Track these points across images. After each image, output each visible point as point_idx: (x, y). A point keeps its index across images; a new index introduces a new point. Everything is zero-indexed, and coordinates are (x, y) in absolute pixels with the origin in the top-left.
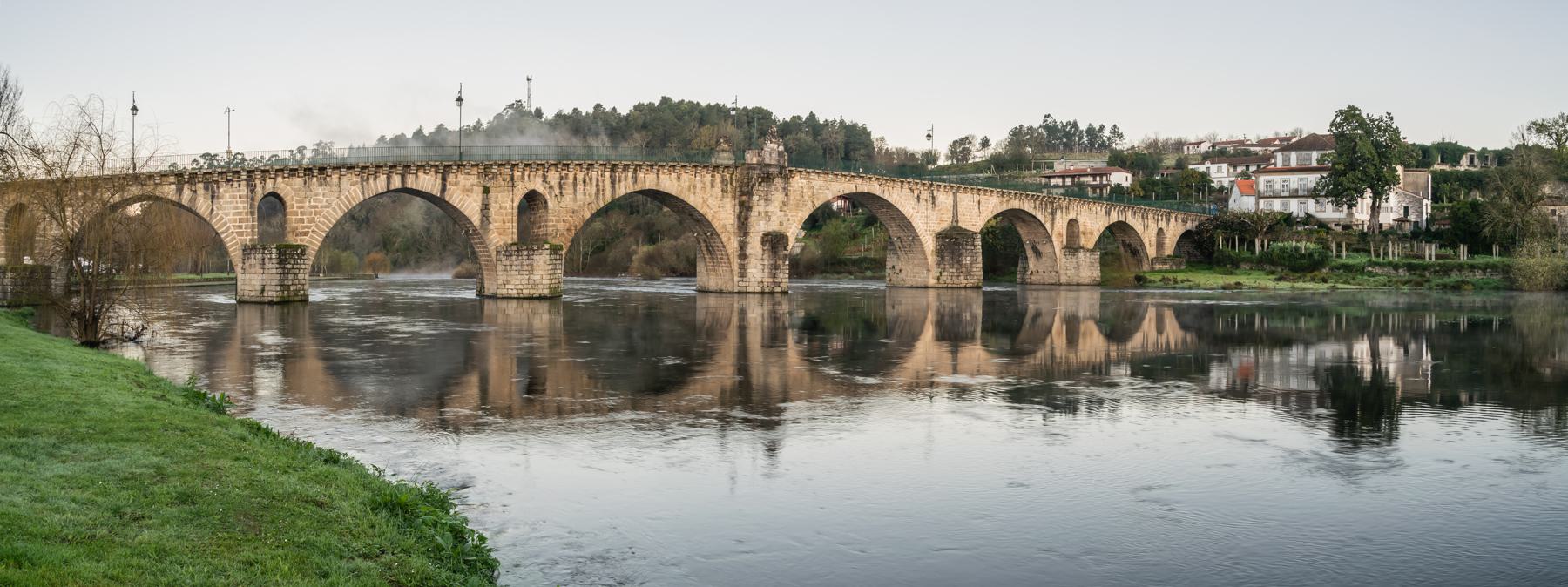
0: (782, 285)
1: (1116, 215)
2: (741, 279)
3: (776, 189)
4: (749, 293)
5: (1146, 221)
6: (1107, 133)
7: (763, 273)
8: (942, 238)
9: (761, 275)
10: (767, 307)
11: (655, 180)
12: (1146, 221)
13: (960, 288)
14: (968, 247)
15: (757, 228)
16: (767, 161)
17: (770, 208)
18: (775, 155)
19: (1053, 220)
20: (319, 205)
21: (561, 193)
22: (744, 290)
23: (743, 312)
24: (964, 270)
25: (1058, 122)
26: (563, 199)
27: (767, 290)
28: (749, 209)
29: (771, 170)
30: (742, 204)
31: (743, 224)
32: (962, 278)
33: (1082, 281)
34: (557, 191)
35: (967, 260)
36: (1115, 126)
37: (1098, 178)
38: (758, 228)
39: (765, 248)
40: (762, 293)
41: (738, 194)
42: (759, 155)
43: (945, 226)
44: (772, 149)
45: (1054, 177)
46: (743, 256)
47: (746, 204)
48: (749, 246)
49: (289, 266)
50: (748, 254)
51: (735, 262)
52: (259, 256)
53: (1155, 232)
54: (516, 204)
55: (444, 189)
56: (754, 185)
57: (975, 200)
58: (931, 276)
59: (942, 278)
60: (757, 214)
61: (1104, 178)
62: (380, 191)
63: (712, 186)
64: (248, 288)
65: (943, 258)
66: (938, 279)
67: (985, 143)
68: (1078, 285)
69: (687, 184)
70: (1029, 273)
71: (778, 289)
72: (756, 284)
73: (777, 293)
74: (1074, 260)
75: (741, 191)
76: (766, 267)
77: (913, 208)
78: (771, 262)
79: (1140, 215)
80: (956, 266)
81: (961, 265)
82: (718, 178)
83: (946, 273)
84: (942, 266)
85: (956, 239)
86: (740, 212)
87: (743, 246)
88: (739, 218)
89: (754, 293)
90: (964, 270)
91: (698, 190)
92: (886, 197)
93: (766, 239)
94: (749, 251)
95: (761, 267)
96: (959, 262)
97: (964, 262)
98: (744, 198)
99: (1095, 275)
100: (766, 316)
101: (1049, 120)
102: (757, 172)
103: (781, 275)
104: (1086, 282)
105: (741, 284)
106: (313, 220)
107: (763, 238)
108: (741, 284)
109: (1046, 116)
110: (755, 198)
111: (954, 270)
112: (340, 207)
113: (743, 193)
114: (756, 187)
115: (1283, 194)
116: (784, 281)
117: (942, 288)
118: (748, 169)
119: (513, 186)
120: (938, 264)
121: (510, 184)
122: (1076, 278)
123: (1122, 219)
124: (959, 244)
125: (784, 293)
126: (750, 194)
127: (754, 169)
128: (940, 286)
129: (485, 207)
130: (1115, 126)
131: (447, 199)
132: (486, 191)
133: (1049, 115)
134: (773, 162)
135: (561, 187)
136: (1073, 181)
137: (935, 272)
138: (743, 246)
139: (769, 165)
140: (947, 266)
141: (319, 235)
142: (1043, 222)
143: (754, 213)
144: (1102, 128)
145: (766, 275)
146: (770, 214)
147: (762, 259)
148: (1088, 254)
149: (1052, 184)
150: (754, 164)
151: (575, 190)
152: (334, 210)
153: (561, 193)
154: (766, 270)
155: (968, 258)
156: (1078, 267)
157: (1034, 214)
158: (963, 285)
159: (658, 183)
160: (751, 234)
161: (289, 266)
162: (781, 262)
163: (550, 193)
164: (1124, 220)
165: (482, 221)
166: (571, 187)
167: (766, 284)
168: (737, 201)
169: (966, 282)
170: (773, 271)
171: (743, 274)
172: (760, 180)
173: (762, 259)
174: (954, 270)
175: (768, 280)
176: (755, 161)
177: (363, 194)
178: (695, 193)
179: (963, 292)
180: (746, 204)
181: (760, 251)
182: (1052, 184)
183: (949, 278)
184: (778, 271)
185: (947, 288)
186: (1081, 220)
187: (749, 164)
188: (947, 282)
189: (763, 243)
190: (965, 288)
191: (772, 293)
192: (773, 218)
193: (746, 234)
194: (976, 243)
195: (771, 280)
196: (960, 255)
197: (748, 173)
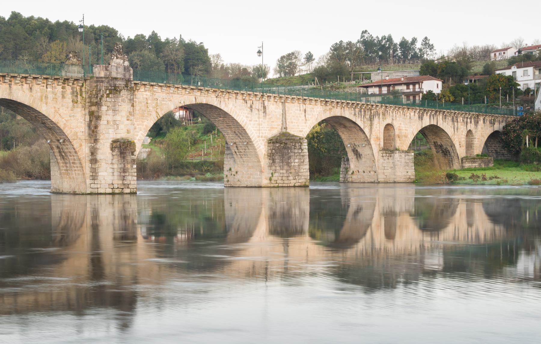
0: (131, 186)
1: (428, 119)
2: (92, 181)
3: (123, 101)
4: (101, 194)
5: (456, 123)
6: (418, 45)
7: (113, 175)
8: (273, 143)
10: (118, 206)
11: (8, 90)
12: (456, 123)
13: (290, 187)
14: (296, 151)
15: (106, 135)
16: (114, 75)
17: (118, 118)
18: (121, 70)
19: (371, 125)
22: (96, 191)
23: (95, 215)
24: (293, 171)
25: (375, 37)
27: (117, 191)
28: (98, 118)
29: (118, 83)
30: (91, 114)
31: (93, 131)
32: (291, 178)
33: (398, 180)
35: (295, 162)
36: (426, 38)
37: (411, 87)
39: (114, 153)
40: (113, 194)
41: (87, 104)
42: (106, 70)
43: (275, 132)
45: (371, 86)
46: (94, 161)
47: (96, 114)
48: (99, 152)
50: (98, 158)
51: (87, 166)
53: (465, 133)
56: (102, 96)
57: (302, 109)
58: (263, 177)
59: (274, 178)
60: (106, 122)
61: (417, 86)
63: (63, 97)
65: (274, 161)
66: (270, 180)
67: (309, 58)
68: (395, 182)
69: (39, 94)
70: (350, 173)
71: (127, 191)
72: (107, 186)
73: (127, 194)
74: (391, 160)
75: (90, 102)
76: (116, 170)
77: (247, 117)
78: (120, 166)
79: (450, 118)
80: (286, 167)
81: (290, 167)
82: (69, 89)
83: (277, 174)
84: (273, 168)
85: (286, 144)
86: (91, 121)
87: (93, 152)
88: (89, 126)
89: (105, 194)
90: (293, 171)
91: (49, 100)
92: (223, 107)
93: (114, 145)
94: (99, 156)
95: (111, 170)
96: (288, 164)
97: (293, 164)
98: (94, 108)
99: (409, 174)
100: (117, 215)
101: (366, 35)
102: (105, 84)
103: (130, 178)
104: (402, 180)
105: (92, 186)
107: (112, 144)
108: (92, 186)
109: (363, 32)
110: (104, 108)
111: (284, 171)
113: (92, 104)
114: (104, 99)
116: (132, 183)
117: (274, 187)
118: (97, 81)
120: (270, 166)
122: (393, 177)
123: (434, 122)
124: (288, 148)
125: (133, 194)
126: (98, 104)
127: (102, 82)
128: (272, 185)
130: (426, 38)
133: (366, 32)
134: (119, 76)
136: (388, 90)
137: (267, 173)
138: (93, 152)
139: (116, 79)
140: (278, 168)
142: (362, 127)
143: (103, 123)
144: (414, 41)
145: (116, 177)
146: (117, 123)
147: (112, 164)
148: (403, 155)
149: (369, 93)
150: (102, 78)
154: (116, 174)
155: (297, 161)
156: (394, 167)
157: (354, 120)
158: (292, 185)
159: (10, 93)
160: (101, 141)
162: (129, 166)
164: (435, 124)
166: (303, 173)
167: (116, 186)
168: (87, 111)
169: (295, 181)
170: (123, 174)
171: (94, 177)
172: (108, 92)
173: (112, 164)
174: (284, 171)
175: (117, 182)
176: (102, 75)
178: (46, 104)
179: (292, 190)
180: (96, 114)
181: (110, 156)
182: (369, 93)
183: (280, 178)
184: (127, 174)
185: (278, 187)
186: (396, 124)
187: (97, 78)
188: (278, 182)
189: (112, 149)
190: (294, 187)
191: (122, 194)
192: (121, 126)
193: (96, 141)
194: (303, 147)
195: (121, 182)
196: (289, 158)
197: (97, 86)
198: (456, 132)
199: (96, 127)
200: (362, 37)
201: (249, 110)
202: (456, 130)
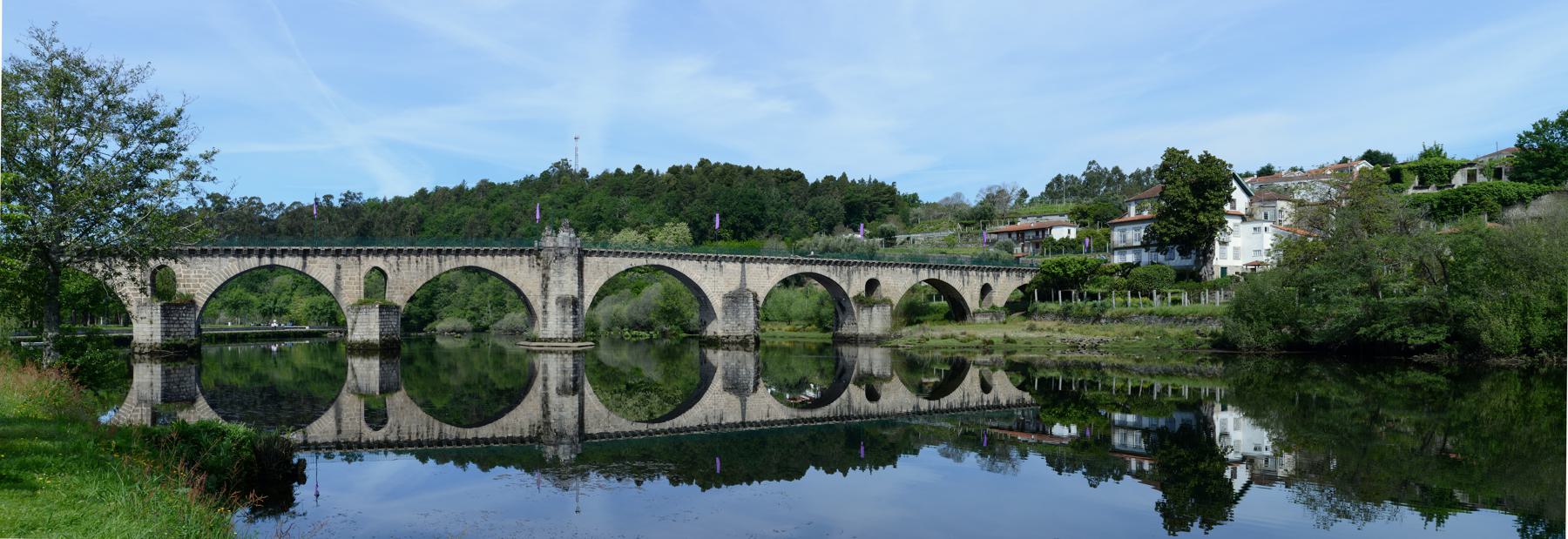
3: (568, 265)
5: (966, 278)
9: (556, 326)
12: (966, 278)
16: (561, 245)
17: (563, 278)
20: (203, 275)
21: (398, 269)
26: (400, 273)
28: (548, 279)
29: (563, 251)
30: (544, 276)
34: (395, 267)
35: (743, 315)
37: (1040, 233)
38: (554, 292)
42: (555, 241)
43: (733, 288)
44: (565, 236)
46: (545, 312)
49: (174, 318)
52: (149, 311)
53: (979, 288)
54: (362, 276)
55: (305, 265)
62: (253, 266)
64: (141, 334)
65: (726, 312)
77: (701, 275)
91: (509, 266)
94: (548, 309)
96: (737, 316)
101: (1094, 166)
106: (199, 286)
109: (1090, 163)
110: (552, 271)
112: (220, 277)
115: (1134, 245)
119: (360, 264)
120: (724, 318)
121: (358, 262)
129: (338, 278)
131: (307, 273)
132: (339, 267)
133: (1094, 162)
135: (398, 265)
141: (203, 297)
151: (409, 266)
152: (216, 279)
153: (398, 269)
159: (476, 262)
161: (174, 318)
163: (390, 269)
164: (937, 278)
165: (336, 288)
177: (239, 268)
178: (506, 268)
181: (555, 309)
186: (880, 279)
189: (557, 304)
192: (565, 285)
193: (546, 297)
198: (966, 286)
199: (547, 286)
200: (1089, 168)
201: (704, 269)
202: (966, 283)
